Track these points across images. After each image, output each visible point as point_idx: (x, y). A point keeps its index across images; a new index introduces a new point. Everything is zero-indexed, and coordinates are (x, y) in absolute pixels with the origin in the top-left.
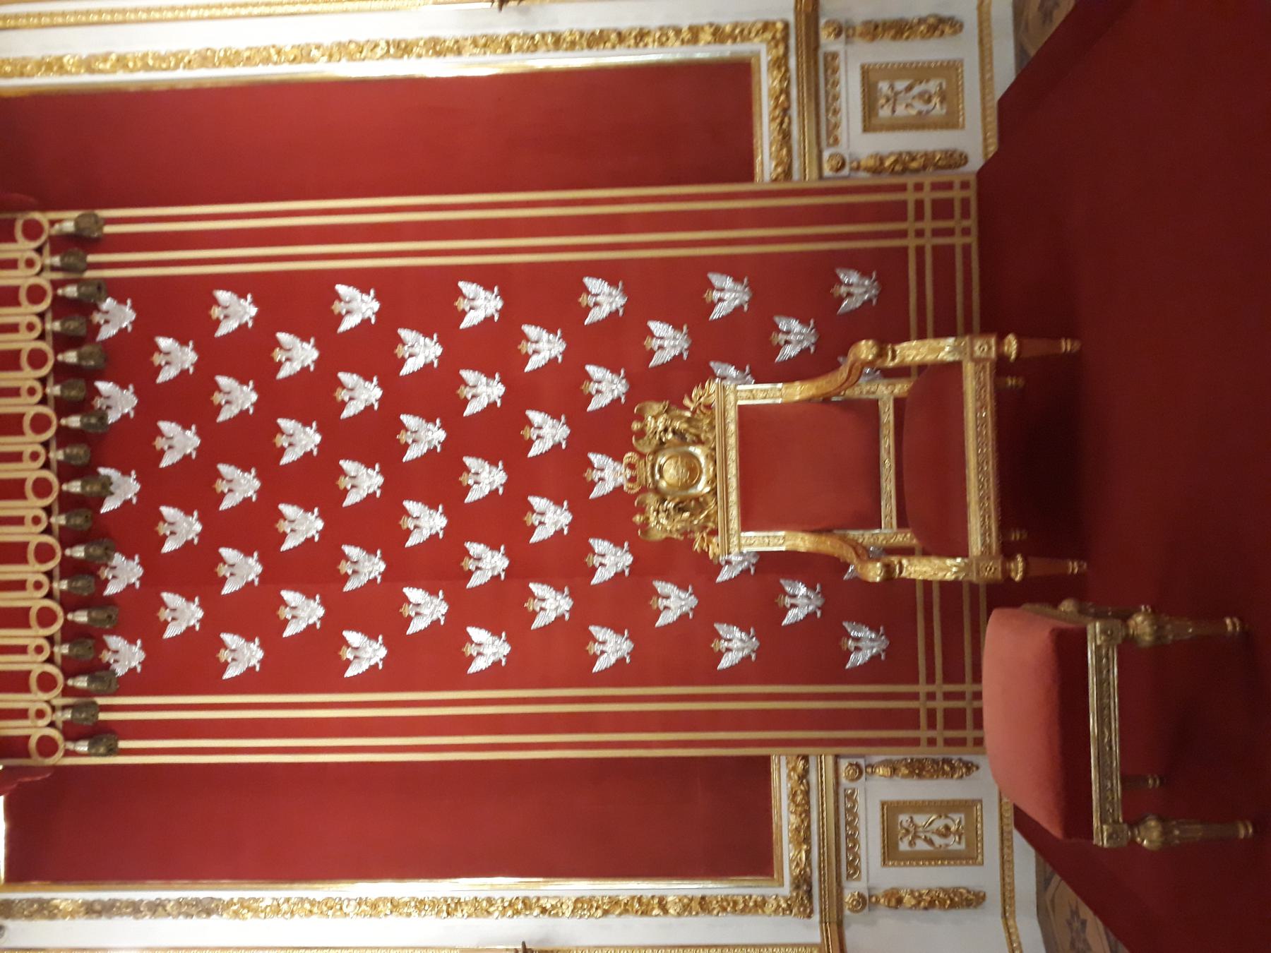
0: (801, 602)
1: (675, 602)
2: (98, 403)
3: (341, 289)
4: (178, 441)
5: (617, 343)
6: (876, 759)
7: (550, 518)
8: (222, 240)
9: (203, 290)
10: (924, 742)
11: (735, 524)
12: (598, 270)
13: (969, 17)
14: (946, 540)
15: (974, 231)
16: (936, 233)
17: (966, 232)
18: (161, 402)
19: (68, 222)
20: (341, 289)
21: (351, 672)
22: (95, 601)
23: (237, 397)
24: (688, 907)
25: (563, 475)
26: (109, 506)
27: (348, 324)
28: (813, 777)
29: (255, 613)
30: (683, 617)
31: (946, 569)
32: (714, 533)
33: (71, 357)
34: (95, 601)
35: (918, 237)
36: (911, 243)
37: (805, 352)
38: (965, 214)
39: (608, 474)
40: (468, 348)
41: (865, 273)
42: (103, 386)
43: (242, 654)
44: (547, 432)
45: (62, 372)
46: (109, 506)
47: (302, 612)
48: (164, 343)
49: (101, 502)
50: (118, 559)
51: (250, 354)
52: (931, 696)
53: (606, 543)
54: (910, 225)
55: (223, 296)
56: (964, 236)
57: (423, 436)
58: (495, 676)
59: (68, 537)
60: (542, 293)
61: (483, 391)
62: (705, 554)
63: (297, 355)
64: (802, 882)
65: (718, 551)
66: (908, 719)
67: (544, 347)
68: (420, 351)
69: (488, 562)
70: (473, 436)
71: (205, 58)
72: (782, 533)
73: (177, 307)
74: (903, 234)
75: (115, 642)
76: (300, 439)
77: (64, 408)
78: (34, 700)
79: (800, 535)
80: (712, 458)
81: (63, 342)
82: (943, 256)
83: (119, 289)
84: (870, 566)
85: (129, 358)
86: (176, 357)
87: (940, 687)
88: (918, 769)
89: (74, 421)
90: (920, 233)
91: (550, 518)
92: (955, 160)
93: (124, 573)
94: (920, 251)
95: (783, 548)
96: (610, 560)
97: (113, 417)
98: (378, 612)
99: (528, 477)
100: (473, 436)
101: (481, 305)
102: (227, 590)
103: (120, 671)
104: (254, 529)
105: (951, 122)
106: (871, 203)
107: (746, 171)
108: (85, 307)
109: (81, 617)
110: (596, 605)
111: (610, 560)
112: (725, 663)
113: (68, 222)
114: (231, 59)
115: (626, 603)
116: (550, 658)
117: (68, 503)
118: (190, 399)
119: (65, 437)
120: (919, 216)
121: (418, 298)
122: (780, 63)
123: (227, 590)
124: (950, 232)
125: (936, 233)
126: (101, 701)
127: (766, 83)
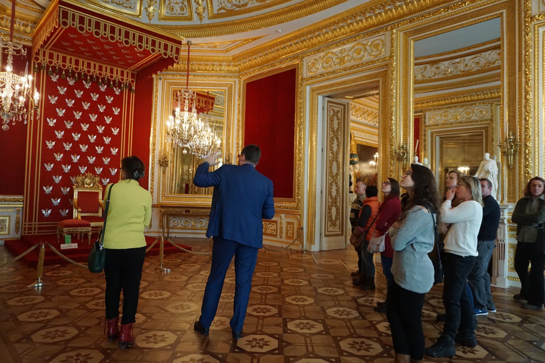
2: (103, 85)
3: (118, 129)
6: (21, 215)
7: (76, 159)
8: (128, 111)
9: (120, 106)
13: (151, 230)
19: (134, 88)
20: (118, 129)
21: (48, 119)
25: (83, 162)
28: (18, 203)
29: (61, 104)
30: (54, 181)
33: (112, 83)
39: (83, 170)
40: (107, 149)
42: (106, 86)
45: (109, 81)
48: (112, 99)
49: (85, 81)
50: (74, 81)
55: (119, 110)
57: (93, 139)
59: (79, 74)
63: (108, 120)
66: (30, 220)
69: (68, 147)
71: (155, 114)
73: (118, 102)
75: (58, 76)
76: (93, 118)
77: (103, 79)
80: (91, 187)
81: (114, 81)
83: (122, 93)
86: (110, 100)
88: (17, 223)
89: (100, 81)
93: (71, 83)
97: (100, 86)
98: (60, 126)
101: (114, 151)
102: (66, 100)
108: (120, 87)
113: (134, 88)
114: (155, 118)
115: (58, 170)
116: (48, 156)
117: (86, 75)
118: (102, 101)
119: (98, 78)
123: (66, 100)
126: (45, 71)
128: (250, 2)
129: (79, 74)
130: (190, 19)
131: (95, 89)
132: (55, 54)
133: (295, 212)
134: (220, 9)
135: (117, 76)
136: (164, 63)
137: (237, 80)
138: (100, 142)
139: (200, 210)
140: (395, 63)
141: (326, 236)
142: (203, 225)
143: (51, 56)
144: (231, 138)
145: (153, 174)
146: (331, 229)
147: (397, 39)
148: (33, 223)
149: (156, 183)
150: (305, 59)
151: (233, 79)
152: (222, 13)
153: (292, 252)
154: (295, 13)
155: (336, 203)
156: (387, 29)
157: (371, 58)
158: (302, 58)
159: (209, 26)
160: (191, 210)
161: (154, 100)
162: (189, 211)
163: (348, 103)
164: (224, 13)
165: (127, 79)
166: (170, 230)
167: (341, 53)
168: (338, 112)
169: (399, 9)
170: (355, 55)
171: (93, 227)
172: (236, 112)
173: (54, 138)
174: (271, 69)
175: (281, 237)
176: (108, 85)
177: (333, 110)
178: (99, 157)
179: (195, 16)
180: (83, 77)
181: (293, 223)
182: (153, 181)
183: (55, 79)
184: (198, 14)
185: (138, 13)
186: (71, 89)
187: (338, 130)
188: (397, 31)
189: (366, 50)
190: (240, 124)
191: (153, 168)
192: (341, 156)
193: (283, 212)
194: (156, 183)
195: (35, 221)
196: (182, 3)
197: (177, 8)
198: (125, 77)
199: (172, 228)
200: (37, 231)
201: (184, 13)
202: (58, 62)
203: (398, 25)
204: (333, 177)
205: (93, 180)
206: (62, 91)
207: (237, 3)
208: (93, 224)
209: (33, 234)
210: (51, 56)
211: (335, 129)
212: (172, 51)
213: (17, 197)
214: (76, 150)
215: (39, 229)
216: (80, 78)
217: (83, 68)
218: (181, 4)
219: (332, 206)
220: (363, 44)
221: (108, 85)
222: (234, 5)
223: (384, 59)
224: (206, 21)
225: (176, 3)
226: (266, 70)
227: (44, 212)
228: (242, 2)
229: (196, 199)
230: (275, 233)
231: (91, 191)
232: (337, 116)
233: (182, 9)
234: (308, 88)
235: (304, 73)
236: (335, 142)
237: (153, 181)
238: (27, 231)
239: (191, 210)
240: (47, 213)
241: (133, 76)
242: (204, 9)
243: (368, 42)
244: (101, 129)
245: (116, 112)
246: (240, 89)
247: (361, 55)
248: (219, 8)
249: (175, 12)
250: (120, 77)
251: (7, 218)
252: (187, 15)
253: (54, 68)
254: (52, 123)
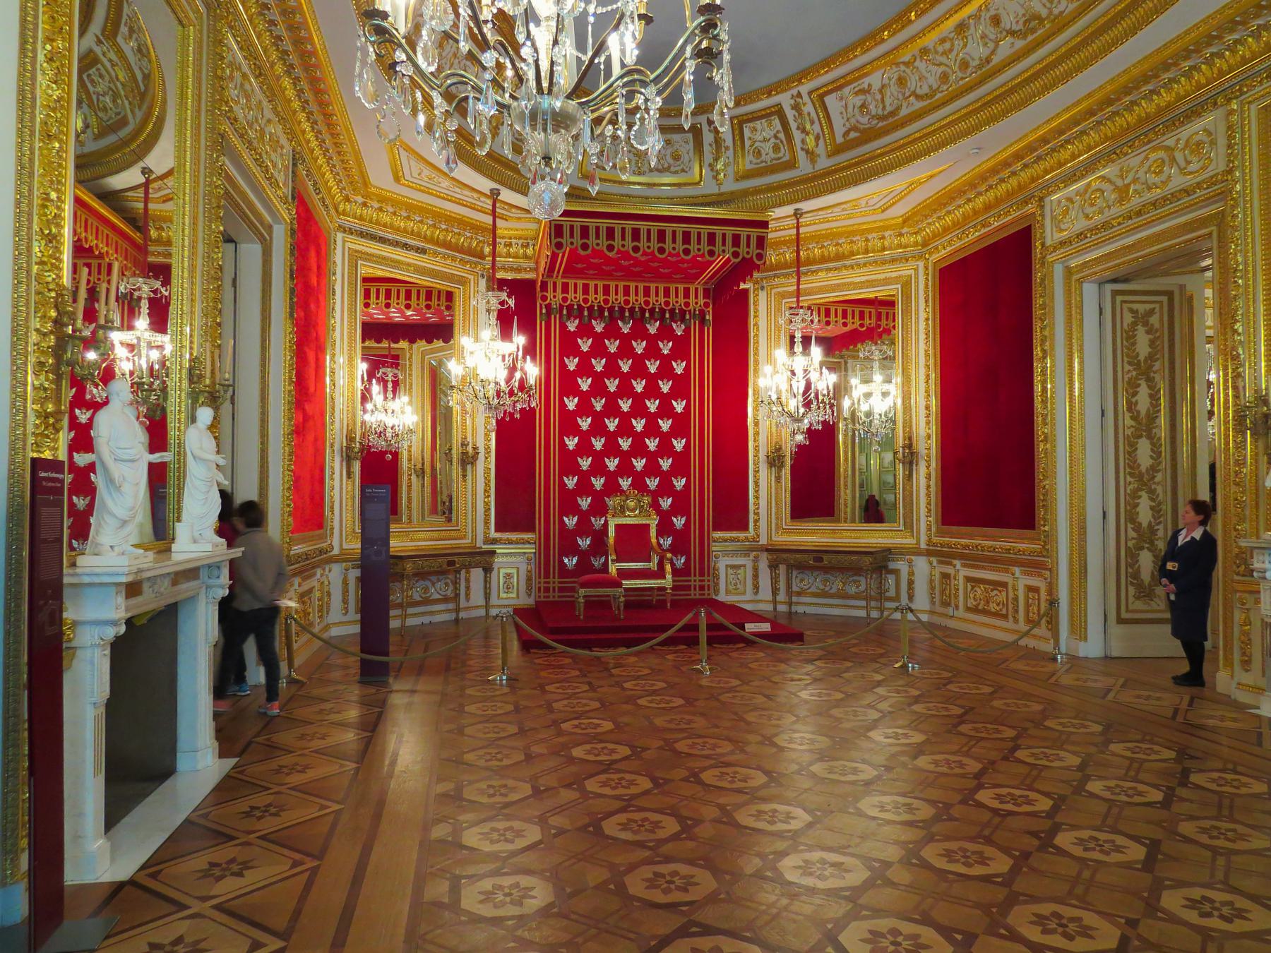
0: (584, 543)
4: (640, 347)
5: (666, 488)
7: (612, 464)
8: (701, 365)
12: (688, 482)
18: (652, 341)
19: (709, 317)
22: (591, 317)
23: (653, 367)
24: (487, 504)
26: (620, 323)
27: (674, 403)
33: (667, 315)
34: (591, 317)
35: (694, 580)
39: (625, 483)
40: (665, 440)
43: (572, 364)
44: (639, 464)
45: (663, 311)
46: (620, 323)
47: (585, 384)
50: (603, 325)
51: (666, 371)
54: (698, 578)
58: (563, 445)
59: (611, 310)
60: (682, 464)
61: (652, 444)
63: (665, 387)
64: (494, 541)
66: (547, 575)
67: (665, 464)
68: (665, 425)
70: (638, 440)
73: (681, 350)
77: (652, 311)
78: (560, 296)
81: (672, 311)
83: (687, 330)
85: (666, 333)
87: (557, 585)
88: (529, 579)
91: (612, 464)
92: (717, 592)
93: (599, 327)
96: (598, 483)
98: (585, 408)
99: (626, 458)
100: (638, 440)
101: (679, 445)
103: (568, 324)
104: (612, 370)
105: (727, 592)
106: (704, 566)
107: (716, 528)
108: (683, 320)
109: (586, 313)
110: (584, 478)
111: (598, 483)
113: (709, 317)
115: (584, 487)
116: (568, 463)
117: (622, 310)
118: (652, 352)
119: (642, 311)
121: (681, 426)
122: (747, 539)
127: (742, 535)
128: (905, 105)
129: (611, 310)
130: (791, 165)
131: (639, 331)
132: (571, 282)
133: (1039, 564)
134: (846, 133)
135: (677, 301)
136: (746, 268)
137: (921, 264)
138: (652, 429)
139: (848, 558)
140: (1238, 187)
141: (1120, 621)
142: (862, 588)
143: (565, 288)
144: (913, 397)
145: (756, 483)
146: (1139, 605)
147: (1242, 126)
148: (551, 580)
149: (763, 503)
150: (1047, 200)
151: (912, 263)
152: (852, 140)
153: (1033, 654)
154: (995, 109)
155: (1152, 542)
156: (1215, 104)
157: (1190, 180)
158: (1041, 199)
159: (828, 173)
160: (825, 557)
161: (752, 334)
162: (821, 560)
163: (1182, 287)
164: (856, 138)
165: (697, 302)
166: (794, 599)
167: (1121, 177)
168: (1152, 312)
169: (1217, 60)
170: (1152, 178)
171: (626, 589)
172: (922, 336)
173: (575, 430)
174: (983, 231)
175: (1016, 621)
176: (662, 319)
177: (1131, 311)
178: (652, 458)
179: (801, 156)
180: (617, 315)
181: (1035, 590)
182: (757, 497)
183: (572, 326)
184: (807, 152)
185: (697, 178)
186: (598, 340)
187: (1151, 358)
188: (1242, 104)
189: (1173, 160)
190: (931, 362)
191: (756, 472)
192: (1163, 420)
193: (1015, 563)
194: (763, 503)
196: (776, 137)
197: (767, 148)
198: (692, 300)
199: (799, 594)
200: (557, 594)
201: (781, 155)
202: (575, 297)
203: (1240, 90)
204: (1140, 477)
206: (585, 345)
207: (880, 112)
208: (627, 583)
210: (565, 288)
211: (1142, 358)
212: (748, 246)
213: (526, 536)
214: (612, 448)
215: (561, 590)
216: (614, 316)
217: (617, 299)
218: (773, 140)
219: (1142, 548)
220: (1167, 148)
221: (662, 319)
222: (873, 117)
223: (1212, 181)
224: (824, 163)
225: (765, 140)
226: (974, 235)
227: (566, 561)
228: (889, 109)
229: (845, 534)
230: (1004, 612)
232: (1146, 324)
233: (776, 148)
234: (1058, 270)
235: (1049, 234)
236: (1144, 391)
237: (757, 497)
238: (542, 594)
239: (825, 557)
240: (571, 562)
241: (706, 293)
242: (817, 138)
243: (1179, 140)
244: (653, 406)
245: (679, 368)
246: (927, 285)
247: (1164, 177)
248: (844, 129)
249: (764, 157)
250: (682, 300)
251: (514, 571)
252: (787, 158)
253: (570, 308)
254: (571, 404)
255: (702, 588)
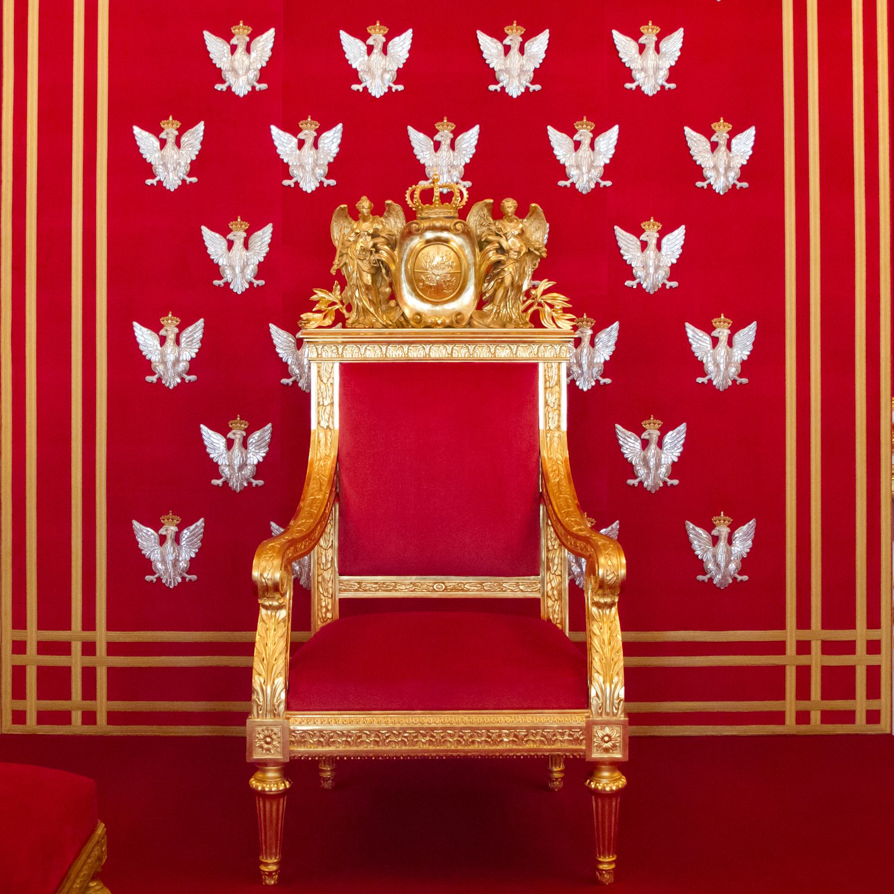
1: (238, 257)
10: (19, 635)
11: (353, 354)
14: (318, 674)
15: (803, 729)
16: (804, 673)
17: (803, 717)
31: (270, 677)
32: (340, 319)
35: (799, 642)
36: (791, 634)
37: (629, 470)
38: (828, 717)
39: (445, 157)
41: (746, 564)
52: (89, 648)
53: (335, 150)
54: (817, 633)
56: (798, 714)
62: (310, 306)
65: (312, 326)
72: (336, 425)
74: (804, 622)
79: (334, 453)
82: (769, 683)
84: (277, 562)
90: (803, 647)
94: (779, 648)
95: (314, 426)
96: (308, 157)
111: (308, 157)
112: (144, 336)
115: (239, 179)
120: (829, 648)
124: (803, 693)
125: (804, 673)
148: (76, 633)
195: (89, 623)
200: (102, 705)
205: (481, 244)
209: (76, 726)
215: (123, 683)
231: (460, 354)
255: (839, 682)
